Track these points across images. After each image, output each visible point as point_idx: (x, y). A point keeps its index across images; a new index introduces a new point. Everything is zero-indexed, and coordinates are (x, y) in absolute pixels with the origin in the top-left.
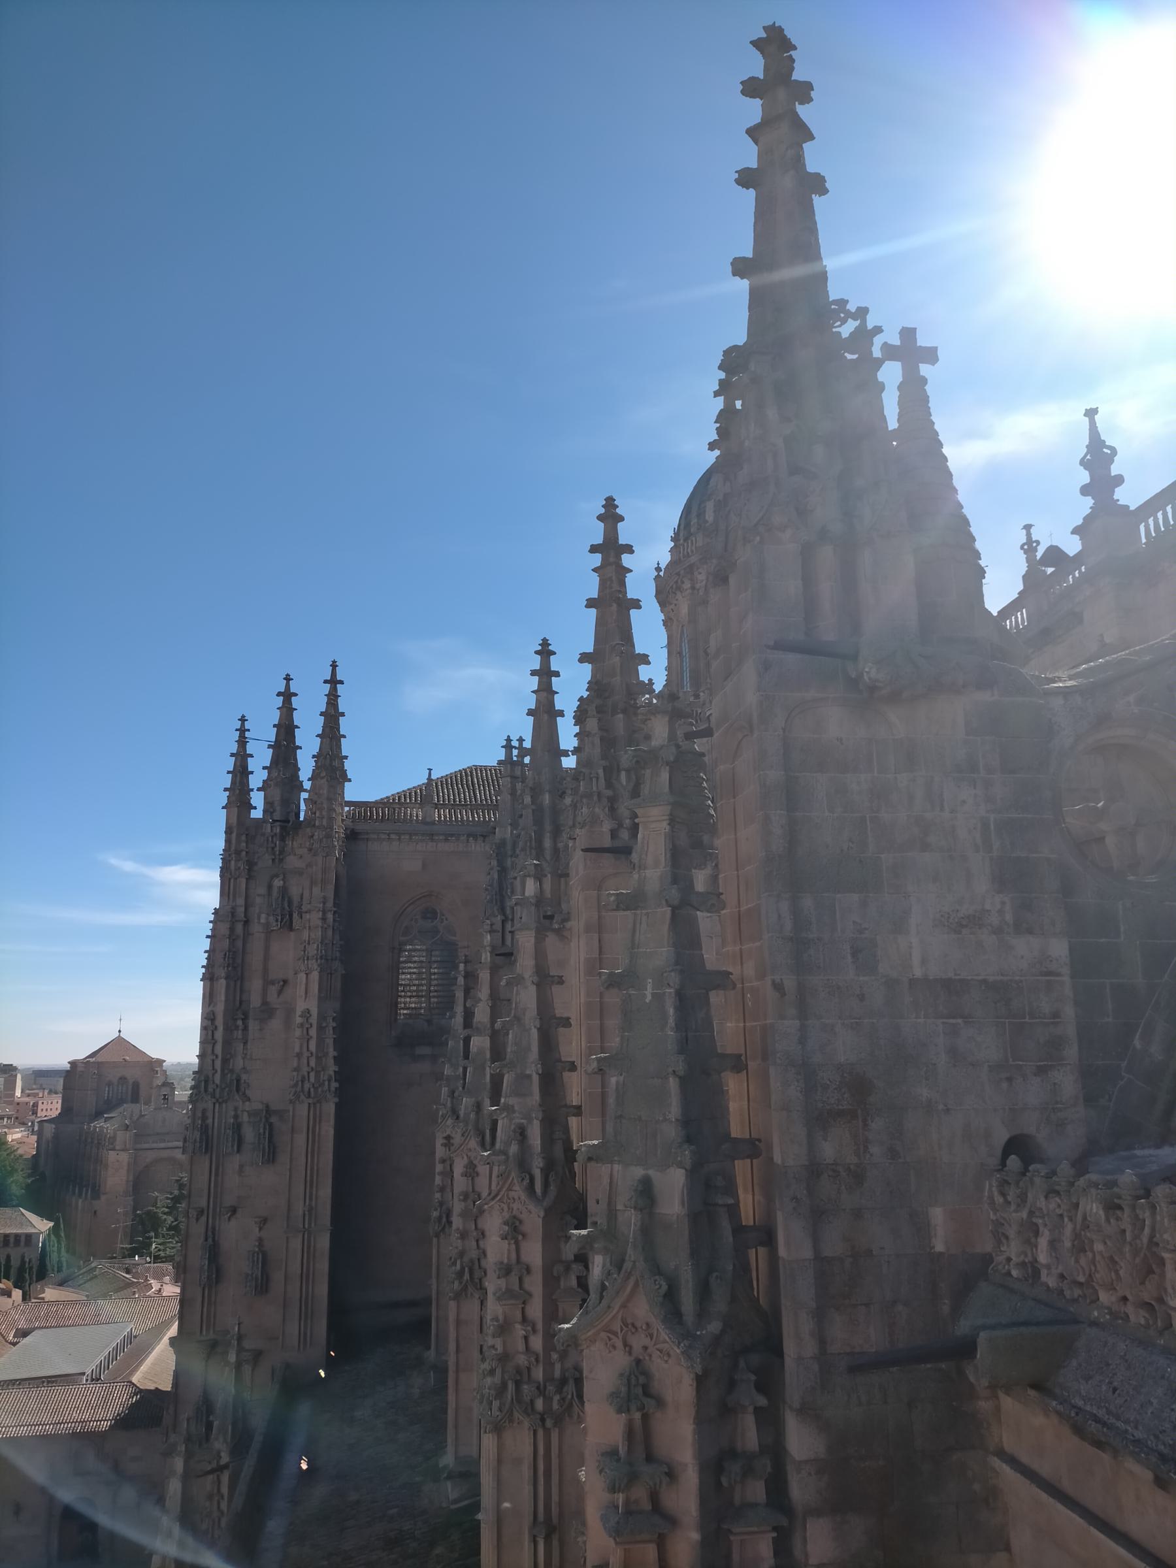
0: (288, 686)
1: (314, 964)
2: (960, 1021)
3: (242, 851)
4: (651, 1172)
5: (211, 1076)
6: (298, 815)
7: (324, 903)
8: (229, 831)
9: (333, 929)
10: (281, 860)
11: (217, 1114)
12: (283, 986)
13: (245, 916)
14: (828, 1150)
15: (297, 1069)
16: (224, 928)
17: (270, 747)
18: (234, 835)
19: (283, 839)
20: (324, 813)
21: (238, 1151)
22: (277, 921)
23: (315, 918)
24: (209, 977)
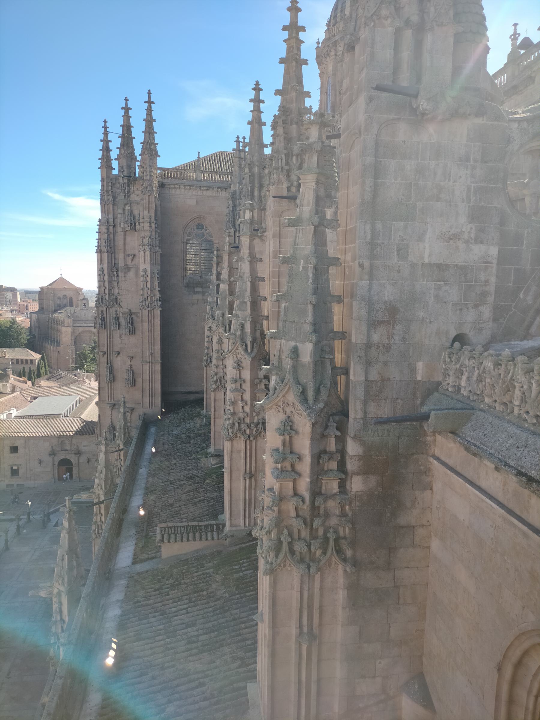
0: (126, 104)
1: (147, 248)
2: (442, 283)
4: (298, 344)
5: (104, 296)
6: (135, 174)
7: (150, 219)
8: (102, 180)
10: (129, 196)
11: (108, 313)
13: (114, 223)
14: (376, 337)
15: (142, 295)
16: (104, 229)
17: (119, 137)
18: (105, 183)
19: (129, 186)
20: (148, 173)
21: (119, 329)
22: (128, 226)
23: (146, 225)
24: (99, 251)
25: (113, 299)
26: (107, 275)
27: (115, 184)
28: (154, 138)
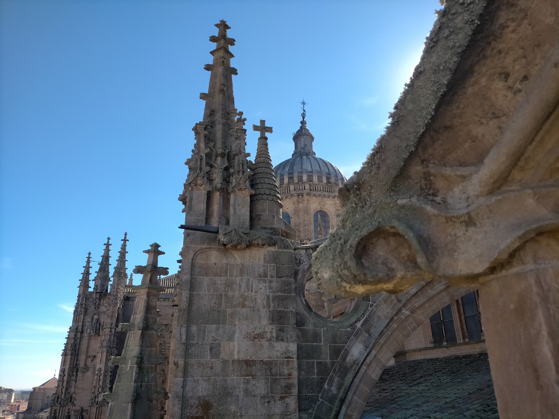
1: (105, 350)
3: (83, 304)
5: (60, 395)
6: (107, 290)
7: (111, 325)
8: (79, 296)
9: (114, 336)
10: (98, 308)
12: (94, 358)
15: (93, 393)
16: (73, 335)
18: (81, 298)
20: (115, 290)
22: (94, 332)
23: (107, 331)
24: (65, 355)
25: (68, 397)
26: (66, 375)
27: (89, 299)
28: (125, 265)
